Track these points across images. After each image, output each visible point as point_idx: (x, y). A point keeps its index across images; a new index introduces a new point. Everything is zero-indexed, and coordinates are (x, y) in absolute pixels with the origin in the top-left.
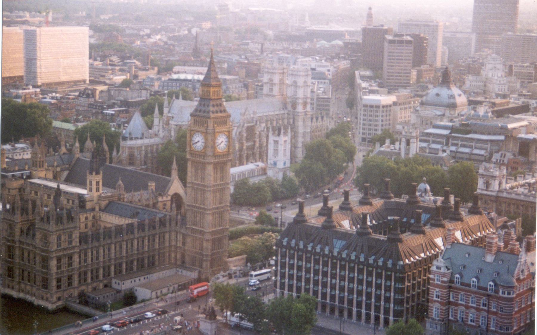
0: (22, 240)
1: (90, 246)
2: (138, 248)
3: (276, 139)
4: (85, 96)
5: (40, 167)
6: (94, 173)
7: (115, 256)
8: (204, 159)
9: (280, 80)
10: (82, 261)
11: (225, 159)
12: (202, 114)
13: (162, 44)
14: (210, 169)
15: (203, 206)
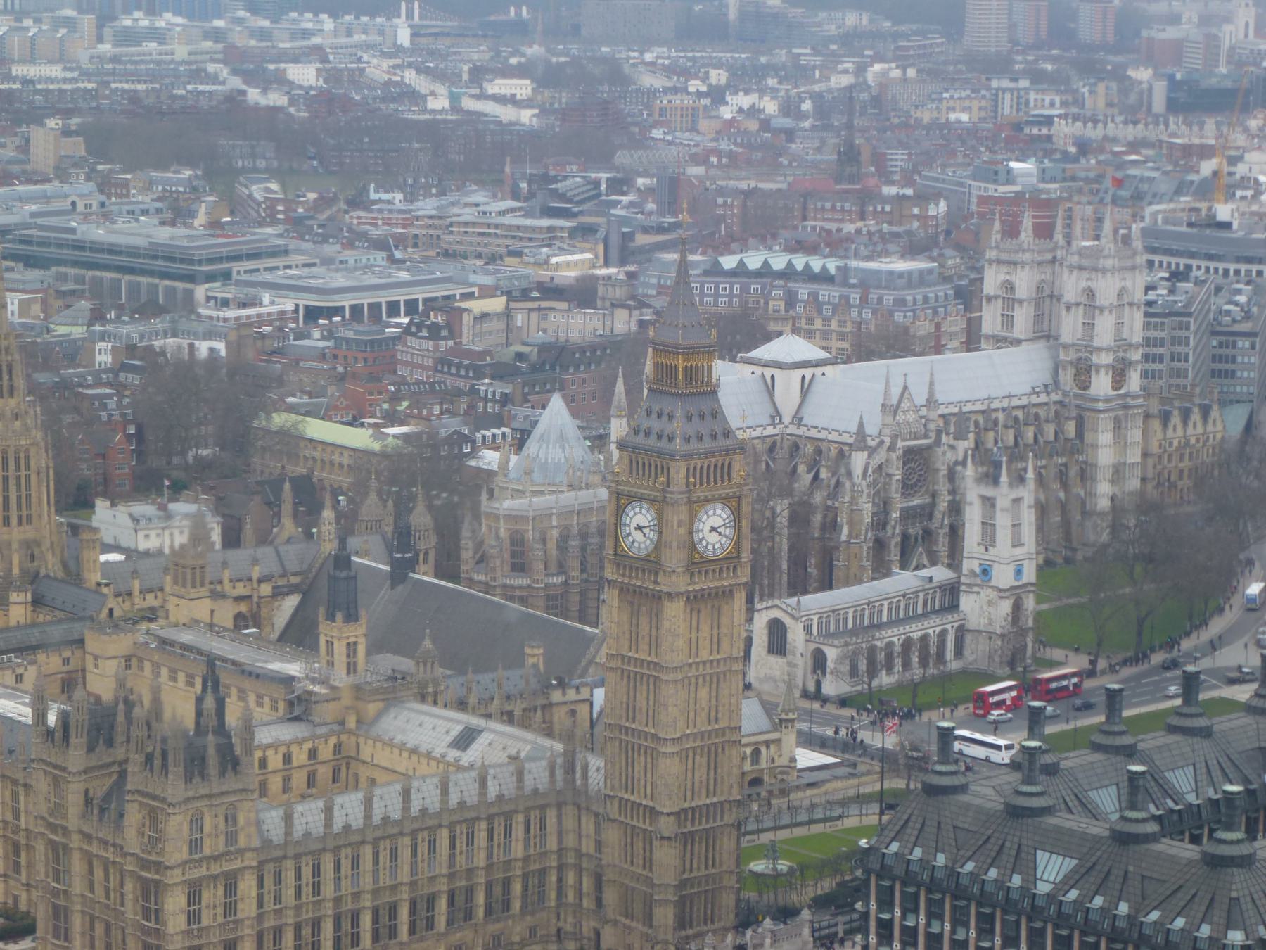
0: (85, 829)
1: (291, 852)
2: (452, 856)
3: (989, 492)
4: (424, 333)
5: (194, 586)
6: (339, 616)
7: (376, 880)
8: (656, 582)
9: (1039, 289)
10: (266, 898)
11: (726, 583)
12: (652, 442)
13: (753, 126)
14: (674, 612)
15: (653, 731)
